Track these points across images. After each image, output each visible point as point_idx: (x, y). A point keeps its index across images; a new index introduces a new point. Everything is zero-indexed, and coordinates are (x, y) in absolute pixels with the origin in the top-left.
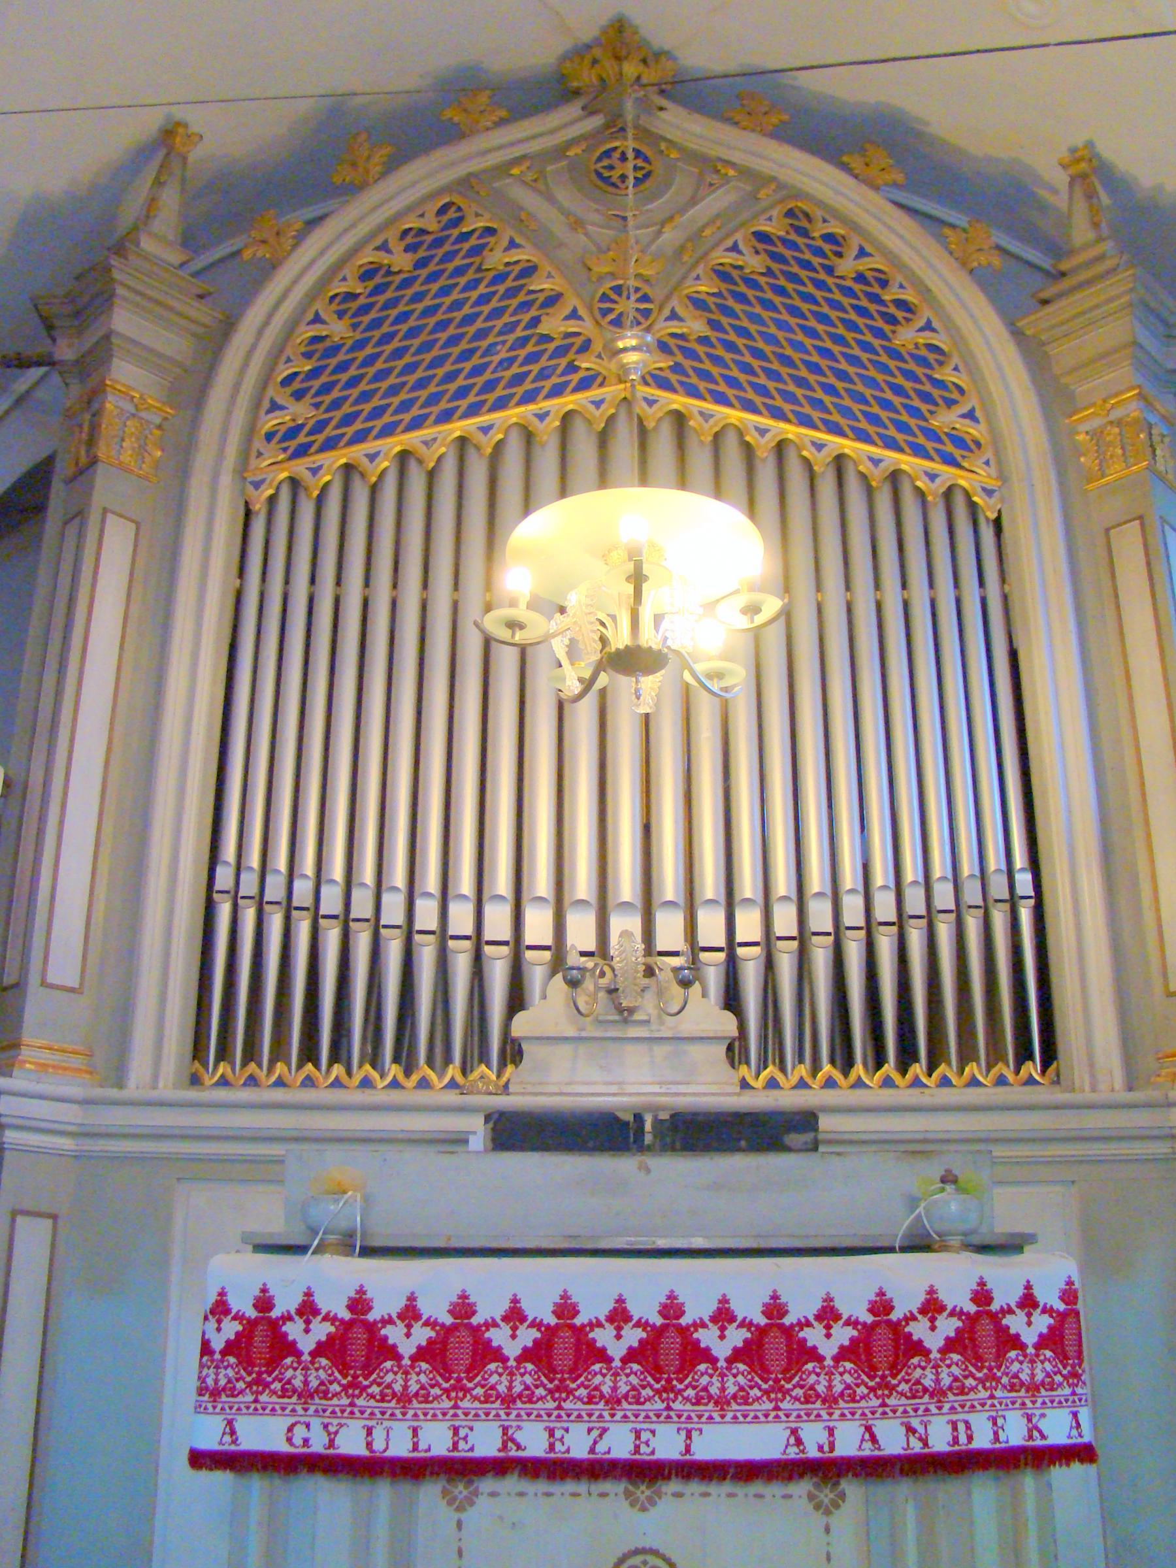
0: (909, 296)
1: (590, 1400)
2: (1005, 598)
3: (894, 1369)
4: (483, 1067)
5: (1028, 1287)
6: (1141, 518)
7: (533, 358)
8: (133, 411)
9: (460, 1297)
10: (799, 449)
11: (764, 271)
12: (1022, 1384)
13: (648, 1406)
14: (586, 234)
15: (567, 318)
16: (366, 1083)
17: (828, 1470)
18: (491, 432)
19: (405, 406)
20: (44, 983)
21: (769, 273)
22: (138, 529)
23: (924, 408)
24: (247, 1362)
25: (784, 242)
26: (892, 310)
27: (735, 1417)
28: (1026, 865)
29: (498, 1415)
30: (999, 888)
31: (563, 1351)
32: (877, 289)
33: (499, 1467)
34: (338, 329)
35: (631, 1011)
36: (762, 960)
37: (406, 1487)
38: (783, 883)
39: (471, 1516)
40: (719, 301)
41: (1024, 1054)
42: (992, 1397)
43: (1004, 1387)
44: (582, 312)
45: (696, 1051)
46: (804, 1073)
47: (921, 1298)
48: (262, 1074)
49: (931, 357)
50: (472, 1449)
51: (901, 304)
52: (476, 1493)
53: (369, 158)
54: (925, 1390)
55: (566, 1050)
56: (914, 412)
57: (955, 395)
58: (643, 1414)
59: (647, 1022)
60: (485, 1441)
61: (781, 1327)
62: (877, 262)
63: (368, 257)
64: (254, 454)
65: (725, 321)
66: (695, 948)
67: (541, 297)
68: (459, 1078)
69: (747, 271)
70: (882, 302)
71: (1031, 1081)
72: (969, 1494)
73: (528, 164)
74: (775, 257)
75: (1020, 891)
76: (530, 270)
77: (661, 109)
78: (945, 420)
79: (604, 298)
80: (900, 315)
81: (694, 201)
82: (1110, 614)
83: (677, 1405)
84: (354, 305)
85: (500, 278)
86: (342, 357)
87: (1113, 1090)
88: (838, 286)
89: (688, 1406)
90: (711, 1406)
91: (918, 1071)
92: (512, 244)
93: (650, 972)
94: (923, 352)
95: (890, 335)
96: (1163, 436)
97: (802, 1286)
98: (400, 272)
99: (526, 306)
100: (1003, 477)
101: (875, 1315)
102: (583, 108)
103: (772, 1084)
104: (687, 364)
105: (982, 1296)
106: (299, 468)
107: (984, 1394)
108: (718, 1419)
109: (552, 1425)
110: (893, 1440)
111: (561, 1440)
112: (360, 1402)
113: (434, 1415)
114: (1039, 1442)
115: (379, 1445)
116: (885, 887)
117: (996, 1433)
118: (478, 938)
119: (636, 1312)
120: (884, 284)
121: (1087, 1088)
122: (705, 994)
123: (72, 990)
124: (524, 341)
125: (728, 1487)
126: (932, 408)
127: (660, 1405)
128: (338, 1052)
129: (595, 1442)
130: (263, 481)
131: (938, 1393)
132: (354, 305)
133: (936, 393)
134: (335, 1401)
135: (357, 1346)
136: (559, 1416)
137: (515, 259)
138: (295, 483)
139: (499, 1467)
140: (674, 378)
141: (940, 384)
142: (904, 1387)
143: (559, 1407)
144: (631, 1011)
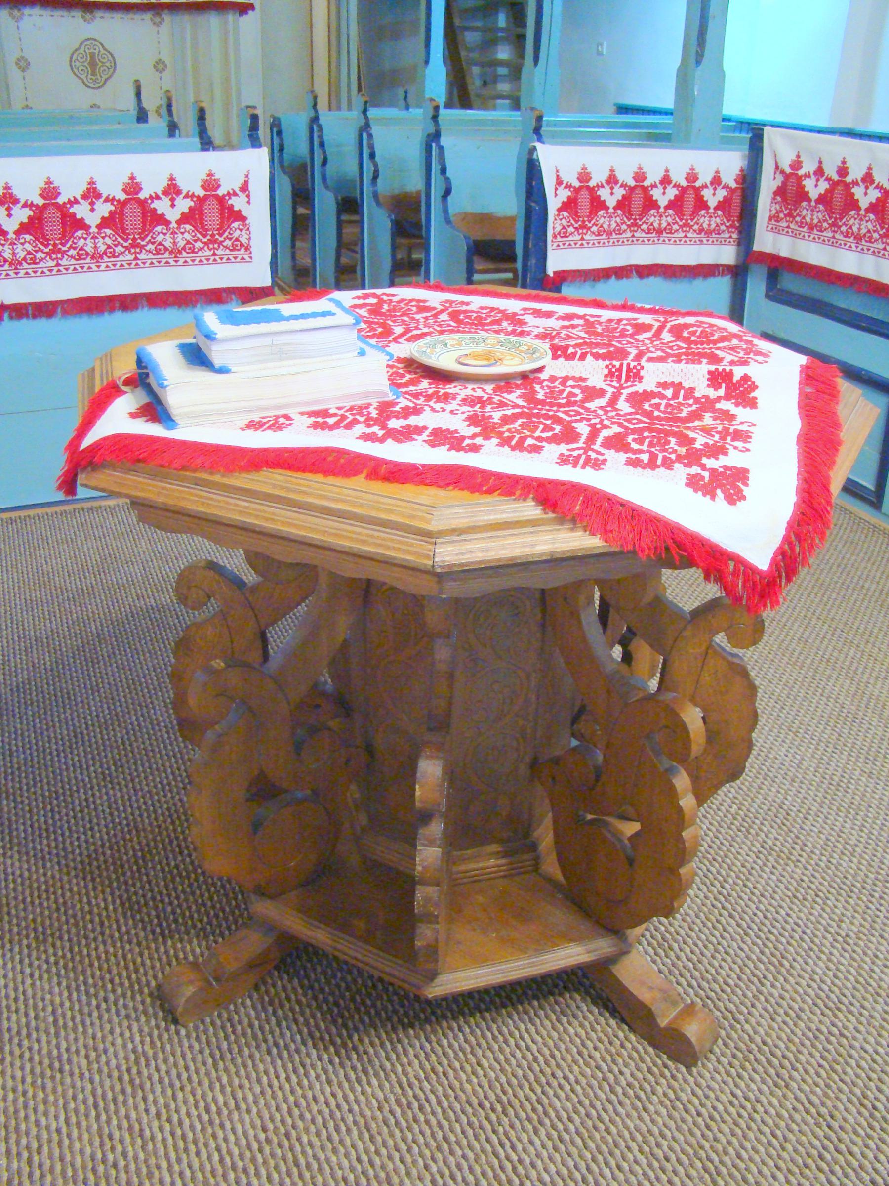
39: (22, 24)
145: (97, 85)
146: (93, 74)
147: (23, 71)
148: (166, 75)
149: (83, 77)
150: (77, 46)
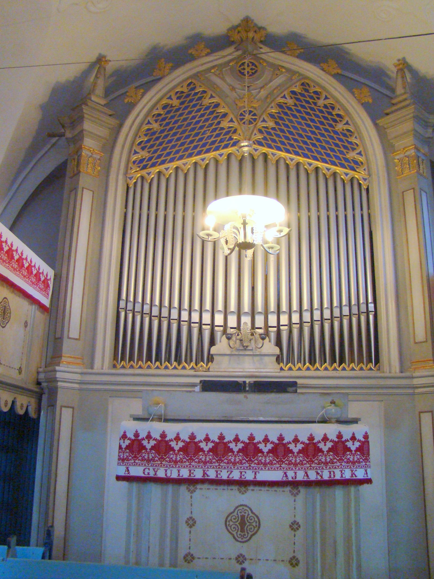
0: (341, 113)
1: (228, 463)
2: (369, 215)
3: (314, 456)
4: (202, 363)
5: (354, 434)
6: (413, 189)
7: (218, 135)
8: (91, 155)
9: (192, 434)
10: (304, 166)
11: (293, 104)
12: (350, 461)
13: (244, 465)
14: (236, 92)
15: (229, 122)
16: (166, 368)
17: (295, 484)
18: (205, 160)
19: (177, 152)
20: (69, 338)
21: (295, 105)
22: (93, 193)
23: (345, 151)
24: (132, 451)
25: (300, 93)
26: (335, 117)
27: (269, 469)
28: (372, 301)
29: (202, 467)
30: (363, 308)
31: (221, 449)
32: (331, 110)
33: (203, 481)
34: (155, 126)
35: (247, 347)
36: (288, 331)
37: (176, 487)
38: (295, 307)
39: (195, 495)
40: (278, 115)
41: (370, 360)
42: (341, 465)
43: (345, 462)
44: (234, 120)
45: (266, 358)
46: (300, 366)
47: (322, 436)
48: (135, 365)
49: (348, 133)
50: (195, 476)
51: (338, 115)
52: (196, 488)
53: (165, 67)
54: (322, 462)
55: (227, 358)
56: (341, 152)
57: (355, 147)
58: (243, 467)
59: (252, 350)
60: (198, 474)
61: (283, 444)
62: (331, 101)
63: (165, 101)
64: (129, 168)
65: (281, 122)
66: (267, 326)
67: (221, 114)
68: (195, 366)
69: (288, 105)
70: (332, 115)
71: (371, 369)
72: (335, 492)
73: (217, 68)
74: (298, 100)
75: (370, 310)
76: (217, 105)
77: (261, 48)
78: (352, 155)
79: (241, 115)
80: (338, 119)
81: (271, 81)
82: (403, 219)
83: (252, 465)
84: (160, 118)
85: (207, 108)
86: (157, 135)
87: (396, 373)
88: (318, 109)
89: (255, 465)
90: (262, 465)
91: (336, 365)
92: (212, 97)
93: (252, 334)
94: (345, 132)
95: (334, 126)
96: (423, 160)
97: (289, 432)
98: (175, 106)
99: (216, 117)
100: (370, 175)
101: (309, 441)
102: (235, 48)
103: (290, 369)
104: (268, 137)
105: (340, 436)
106: (144, 172)
107: (338, 464)
108: (264, 469)
109: (217, 470)
110: (313, 476)
111: (220, 474)
112: (164, 463)
113: (184, 467)
114: (354, 478)
115: (169, 475)
116: (327, 308)
117: (342, 475)
118: (200, 323)
119: (241, 438)
120: (333, 108)
121: (388, 372)
122: (270, 341)
123: (76, 339)
124: (215, 130)
125: (267, 488)
126: (348, 151)
127: (248, 465)
128: (158, 358)
129: (229, 475)
130: (132, 177)
131: (326, 463)
132: (160, 118)
133: (349, 146)
134: (156, 462)
135: (163, 447)
136: (219, 467)
137: (212, 101)
138: (142, 178)
139: (203, 481)
140: (263, 142)
141: (350, 143)
142: (316, 461)
143: (219, 465)
144: (247, 347)
145: (245, 539)
146: (243, 530)
147: (191, 527)
149: (234, 533)
150: (232, 510)
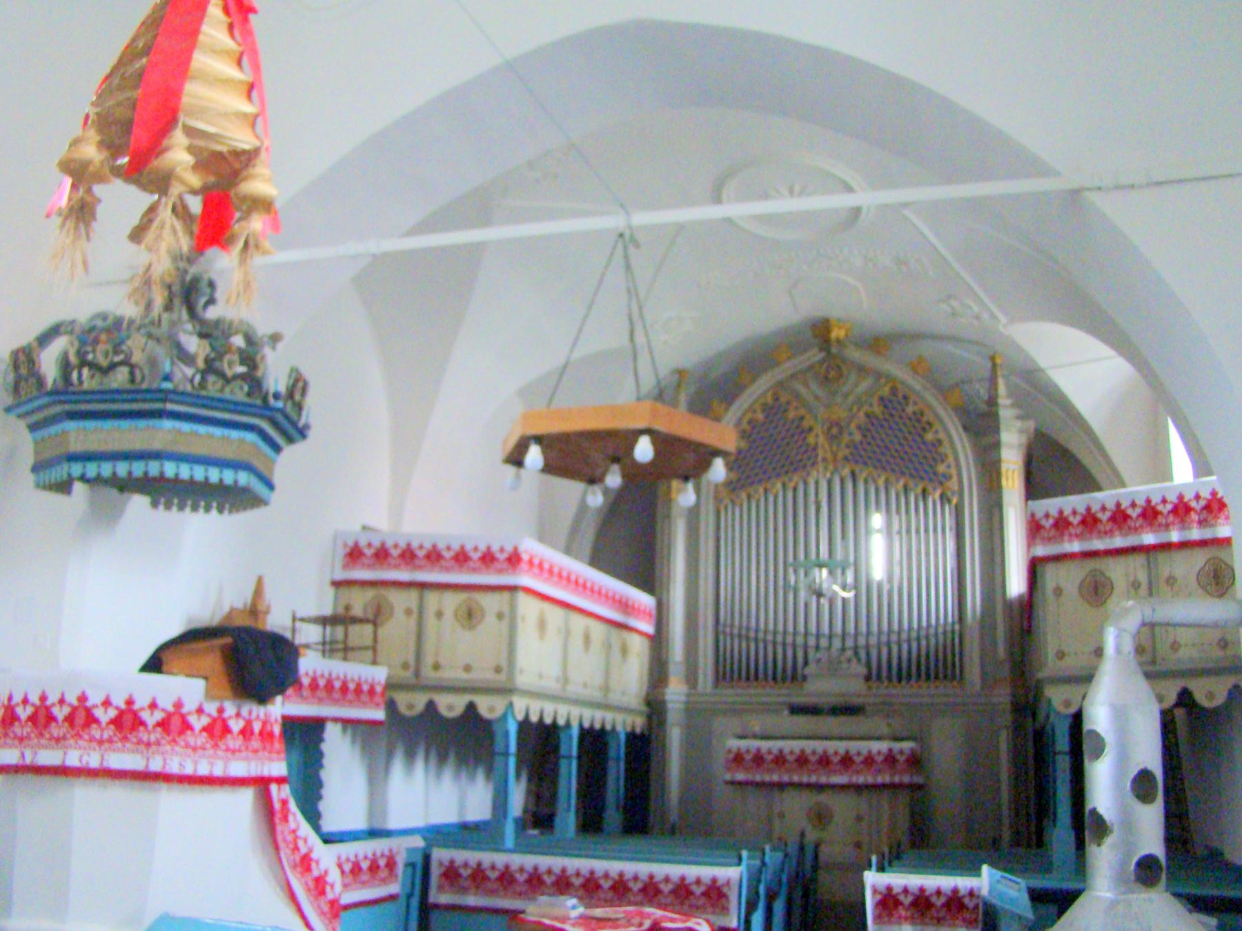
31: (802, 760)
60: (786, 778)
81: (856, 386)
97: (854, 746)
135: (758, 759)
148: (864, 823)
